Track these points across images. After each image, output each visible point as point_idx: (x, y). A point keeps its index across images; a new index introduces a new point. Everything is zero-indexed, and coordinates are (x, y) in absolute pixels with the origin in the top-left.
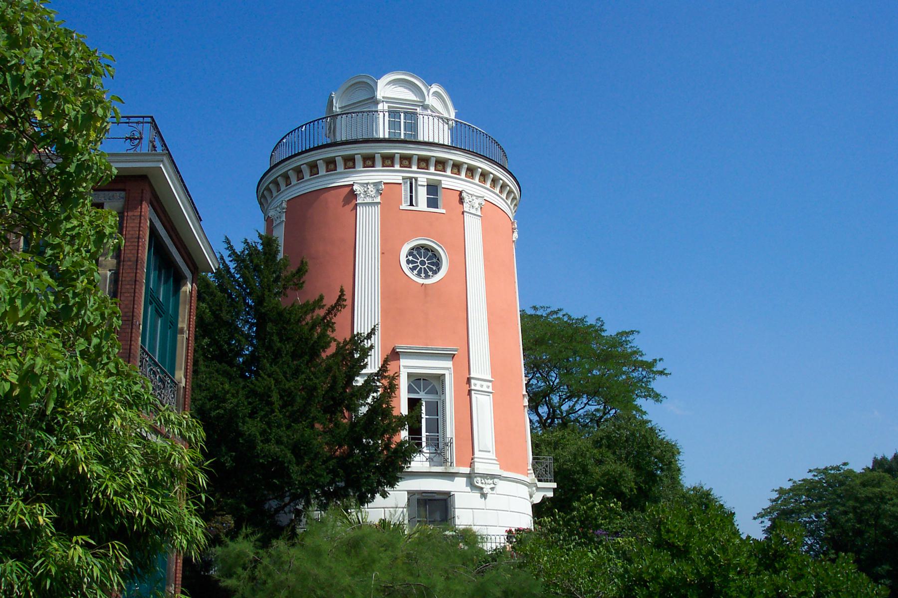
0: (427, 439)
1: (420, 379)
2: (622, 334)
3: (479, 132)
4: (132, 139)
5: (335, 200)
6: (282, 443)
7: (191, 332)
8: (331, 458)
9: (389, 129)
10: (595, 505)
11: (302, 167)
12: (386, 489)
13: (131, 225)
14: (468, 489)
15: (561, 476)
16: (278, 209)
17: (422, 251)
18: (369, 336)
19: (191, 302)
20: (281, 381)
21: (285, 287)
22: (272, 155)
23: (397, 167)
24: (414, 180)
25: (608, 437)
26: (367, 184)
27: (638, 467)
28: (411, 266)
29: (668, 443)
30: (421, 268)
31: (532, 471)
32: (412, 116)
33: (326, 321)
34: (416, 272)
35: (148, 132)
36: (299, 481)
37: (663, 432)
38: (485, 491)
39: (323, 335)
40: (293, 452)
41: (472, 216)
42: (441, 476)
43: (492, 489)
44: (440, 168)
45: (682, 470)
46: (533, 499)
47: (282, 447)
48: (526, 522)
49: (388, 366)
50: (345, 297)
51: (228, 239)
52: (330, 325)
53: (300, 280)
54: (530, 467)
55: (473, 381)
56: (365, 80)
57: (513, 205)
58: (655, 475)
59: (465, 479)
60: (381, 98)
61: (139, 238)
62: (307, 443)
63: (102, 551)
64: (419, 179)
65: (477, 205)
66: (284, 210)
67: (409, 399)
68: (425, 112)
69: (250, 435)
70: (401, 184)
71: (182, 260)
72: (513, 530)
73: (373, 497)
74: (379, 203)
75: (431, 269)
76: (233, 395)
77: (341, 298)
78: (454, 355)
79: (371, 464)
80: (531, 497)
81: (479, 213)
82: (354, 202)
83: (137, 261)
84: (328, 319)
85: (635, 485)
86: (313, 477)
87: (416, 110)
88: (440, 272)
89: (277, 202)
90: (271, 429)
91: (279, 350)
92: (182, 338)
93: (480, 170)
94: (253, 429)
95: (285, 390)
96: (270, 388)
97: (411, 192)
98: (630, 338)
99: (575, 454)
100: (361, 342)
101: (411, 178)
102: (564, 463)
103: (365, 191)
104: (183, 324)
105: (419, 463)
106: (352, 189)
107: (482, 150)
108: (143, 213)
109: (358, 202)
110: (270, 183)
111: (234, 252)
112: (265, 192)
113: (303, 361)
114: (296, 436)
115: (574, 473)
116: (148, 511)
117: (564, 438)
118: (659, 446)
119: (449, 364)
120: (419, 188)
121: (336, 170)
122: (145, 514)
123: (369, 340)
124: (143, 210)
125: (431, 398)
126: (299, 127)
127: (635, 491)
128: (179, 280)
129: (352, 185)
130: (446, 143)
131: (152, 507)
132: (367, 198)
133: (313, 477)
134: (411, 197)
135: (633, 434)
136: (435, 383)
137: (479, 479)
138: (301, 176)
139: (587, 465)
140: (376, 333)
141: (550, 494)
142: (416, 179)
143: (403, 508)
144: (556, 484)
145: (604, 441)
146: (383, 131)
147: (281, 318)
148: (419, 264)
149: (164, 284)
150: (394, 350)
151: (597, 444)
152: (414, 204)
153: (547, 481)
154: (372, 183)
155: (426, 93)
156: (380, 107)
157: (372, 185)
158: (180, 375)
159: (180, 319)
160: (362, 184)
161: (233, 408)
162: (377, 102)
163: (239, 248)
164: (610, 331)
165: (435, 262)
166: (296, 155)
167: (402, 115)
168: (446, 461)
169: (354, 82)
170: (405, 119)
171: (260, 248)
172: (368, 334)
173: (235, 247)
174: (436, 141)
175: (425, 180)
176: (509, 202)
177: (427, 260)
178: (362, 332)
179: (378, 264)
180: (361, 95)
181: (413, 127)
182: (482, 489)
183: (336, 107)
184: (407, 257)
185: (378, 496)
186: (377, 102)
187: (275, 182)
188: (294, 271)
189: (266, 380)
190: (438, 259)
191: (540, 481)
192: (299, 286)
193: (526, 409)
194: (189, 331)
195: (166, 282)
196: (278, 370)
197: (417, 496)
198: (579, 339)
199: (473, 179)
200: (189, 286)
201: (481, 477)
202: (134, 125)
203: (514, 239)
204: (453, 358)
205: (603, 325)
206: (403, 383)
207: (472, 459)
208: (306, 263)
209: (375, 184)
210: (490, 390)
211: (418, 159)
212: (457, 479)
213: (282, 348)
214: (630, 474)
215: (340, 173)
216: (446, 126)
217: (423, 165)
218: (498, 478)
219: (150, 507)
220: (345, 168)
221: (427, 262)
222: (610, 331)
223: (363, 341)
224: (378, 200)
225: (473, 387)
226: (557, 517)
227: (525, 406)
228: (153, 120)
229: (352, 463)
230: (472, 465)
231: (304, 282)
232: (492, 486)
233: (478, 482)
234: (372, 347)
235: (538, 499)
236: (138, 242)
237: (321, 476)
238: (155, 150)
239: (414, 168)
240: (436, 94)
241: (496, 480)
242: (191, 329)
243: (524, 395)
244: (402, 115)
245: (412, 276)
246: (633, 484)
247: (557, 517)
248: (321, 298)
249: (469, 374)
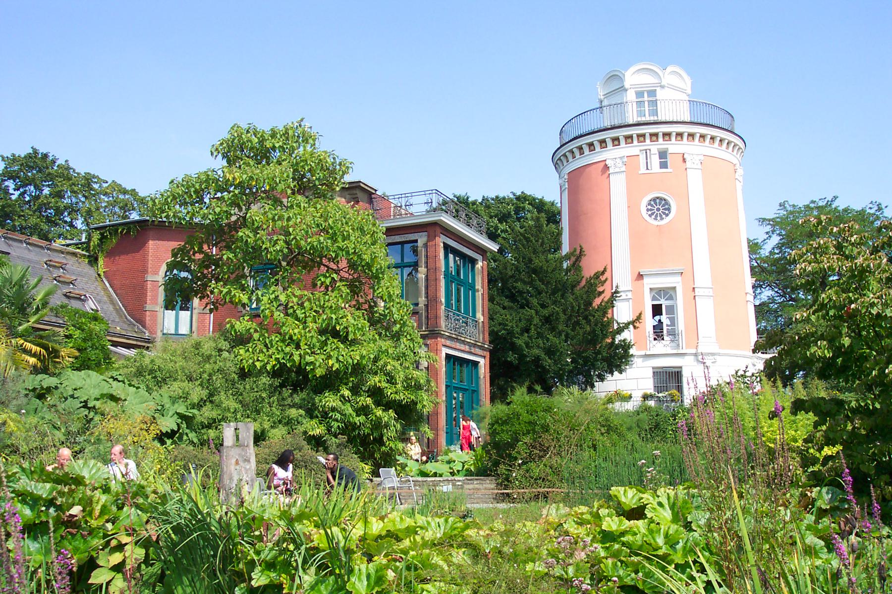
5: (596, 171)
14: (696, 363)
56: (614, 73)
75: (664, 213)
92: (479, 295)
97: (647, 159)
101: (646, 150)
104: (478, 286)
119: (678, 279)
125: (669, 303)
128: (473, 262)
134: (647, 163)
136: (672, 292)
142: (650, 150)
155: (662, 76)
167: (646, 95)
179: (626, 214)
180: (615, 85)
209: (621, 158)
212: (686, 357)
215: (599, 152)
217: (654, 138)
224: (623, 169)
244: (646, 95)
245: (651, 221)
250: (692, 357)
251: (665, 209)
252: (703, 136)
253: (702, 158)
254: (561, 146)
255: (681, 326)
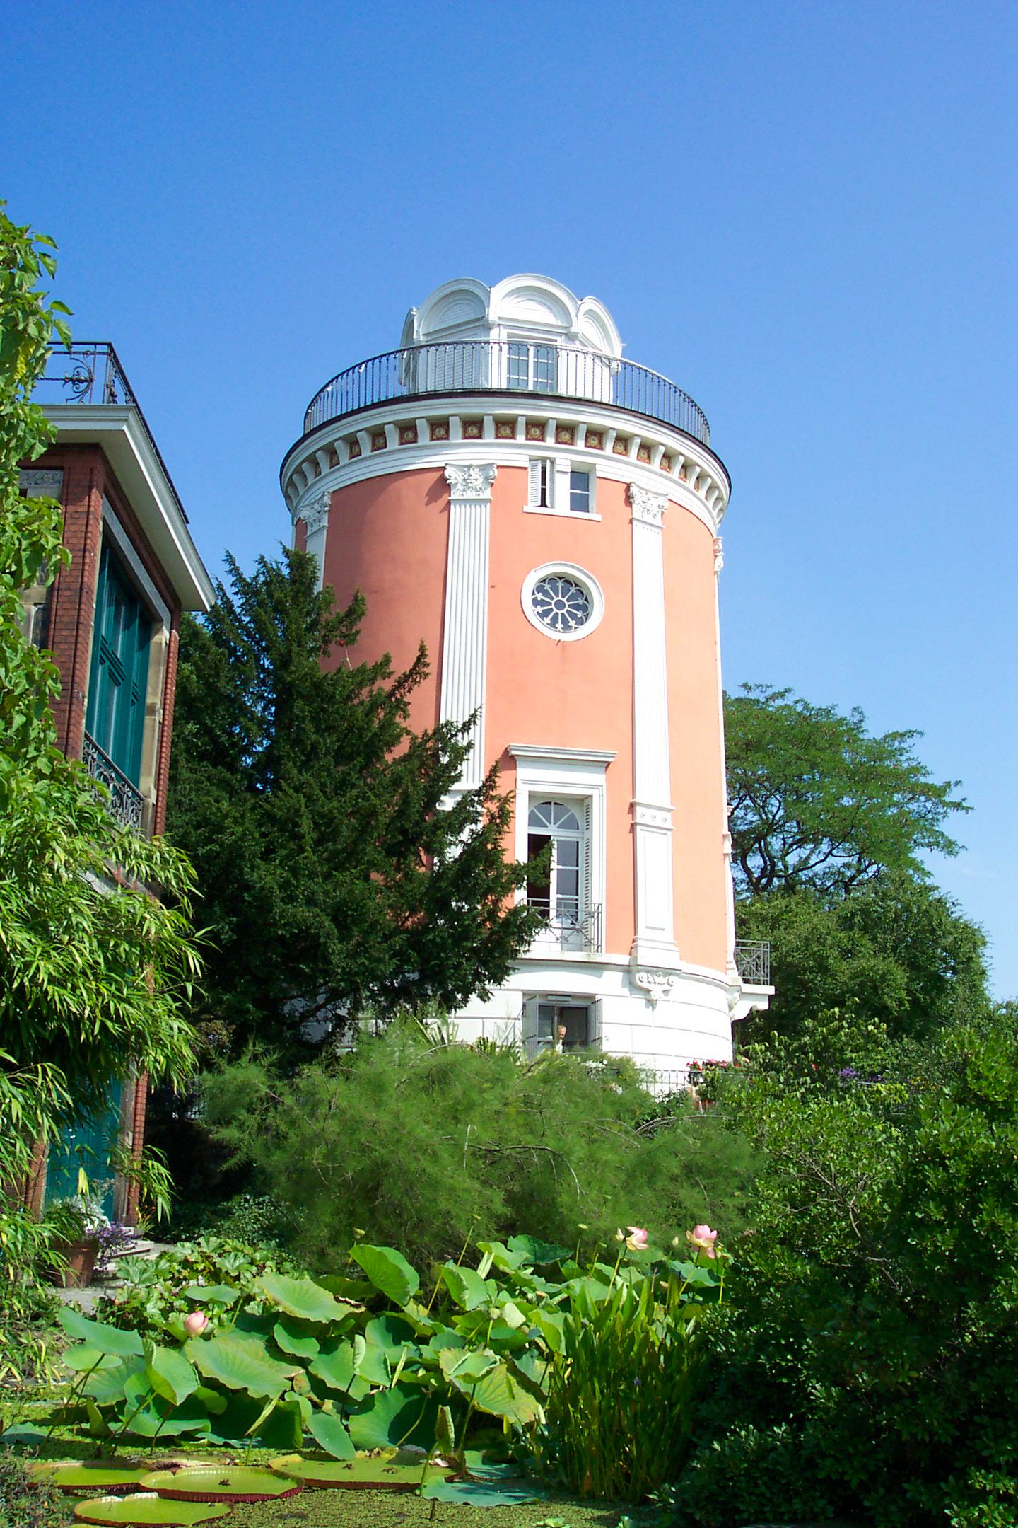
0: (559, 905)
1: (550, 803)
2: (894, 736)
3: (662, 383)
4: (75, 381)
5: (412, 494)
6: (316, 905)
7: (167, 712)
8: (397, 931)
9: (509, 373)
10: (842, 1027)
11: (358, 434)
12: (487, 987)
13: (72, 528)
14: (626, 991)
15: (782, 974)
16: (316, 506)
17: (560, 584)
18: (466, 727)
19: (168, 662)
20: (318, 799)
21: (326, 641)
22: (307, 413)
23: (521, 438)
24: (548, 462)
25: (865, 913)
26: (469, 467)
27: (913, 966)
28: (540, 609)
29: (966, 926)
30: (557, 613)
31: (734, 965)
32: (548, 350)
33: (393, 699)
34: (547, 620)
35: (102, 370)
36: (343, 969)
37: (959, 907)
38: (654, 995)
39: (388, 724)
40: (334, 920)
41: (646, 526)
42: (580, 967)
43: (666, 992)
44: (595, 442)
45: (989, 973)
46: (733, 1012)
47: (316, 910)
48: (722, 1050)
49: (497, 780)
50: (427, 660)
51: (231, 556)
52: (401, 706)
53: (351, 629)
54: (731, 958)
55: (639, 810)
57: (717, 510)
58: (941, 979)
59: (621, 974)
60: (496, 320)
61: (85, 551)
62: (358, 905)
63: (27, 1076)
64: (557, 461)
65: (655, 509)
66: (327, 509)
67: (530, 836)
68: (571, 346)
69: (262, 888)
70: (526, 468)
71: (155, 590)
72: (700, 1063)
73: (465, 1000)
74: (489, 500)
75: (573, 616)
76: (235, 822)
77: (420, 661)
78: (609, 763)
79: (465, 944)
80: (731, 1008)
81: (658, 522)
82: (445, 498)
83: (81, 589)
84: (398, 696)
85: (908, 995)
86: (367, 963)
87: (556, 341)
88: (589, 621)
89: (314, 494)
90: (297, 880)
91: (314, 747)
92: (152, 723)
93: (662, 449)
94: (269, 878)
95: (322, 816)
96: (298, 811)
97: (544, 482)
98: (910, 742)
99: (807, 939)
100: (452, 736)
101: (544, 460)
102: (788, 954)
103: (465, 480)
104: (154, 697)
105: (543, 944)
106: (443, 474)
107: (666, 412)
108: (92, 509)
109: (453, 497)
110: (303, 462)
111: (240, 579)
112: (294, 477)
113: (355, 765)
114: (341, 893)
115: (805, 970)
116: (105, 1011)
117: (790, 911)
118: (952, 930)
119: (598, 778)
120: (558, 476)
121: (416, 442)
122: (99, 1015)
123: (466, 734)
124: (92, 503)
126: (355, 367)
127: (907, 1005)
128: (149, 623)
129: (444, 468)
130: (605, 401)
131: (112, 1004)
132: (469, 491)
133: (367, 963)
134: (543, 491)
135: (907, 909)
136: (575, 811)
137: (644, 975)
138: (355, 450)
139: (828, 957)
140: (478, 722)
141: (763, 1005)
142: (553, 462)
143: (515, 1019)
144: (773, 988)
145: (857, 919)
146: (498, 378)
147: (318, 690)
148: (553, 606)
149: (124, 630)
150: (506, 752)
151: (846, 922)
152: (548, 503)
153: (758, 982)
154: (478, 466)
155: (573, 313)
156: (494, 334)
157: (477, 470)
158: (147, 785)
159: (149, 689)
160: (460, 467)
161: (236, 842)
162: (488, 327)
163: (249, 571)
164: (874, 730)
165: (583, 606)
166: (348, 414)
167: (532, 349)
168: (589, 942)
169: (446, 292)
170: (536, 356)
171: (285, 571)
172: (464, 724)
173: (241, 570)
174: (589, 396)
175: (569, 463)
176: (710, 503)
177: (568, 600)
178: (454, 720)
179: (484, 606)
180: (462, 313)
181: (549, 371)
182: (648, 991)
183: (418, 334)
184: (533, 594)
185: (473, 997)
186: (488, 327)
187: (313, 460)
188: (342, 614)
189: (291, 796)
190: (586, 600)
191: (746, 981)
192: (349, 639)
193: (729, 859)
194: (164, 709)
195: (127, 627)
196: (312, 780)
197: (538, 1001)
198: (822, 743)
199: (649, 463)
200: (166, 633)
201: (648, 972)
202: (80, 357)
203: (717, 569)
204: (607, 767)
205: (862, 721)
206: (521, 810)
207: (634, 941)
208: (363, 599)
209: (483, 468)
210: (668, 825)
211: (558, 427)
212: (606, 974)
213: (319, 743)
214: (900, 975)
216: (606, 370)
217: (565, 436)
218: (678, 975)
219: (108, 1003)
220: (432, 440)
221: (567, 604)
222: (874, 730)
223: (456, 735)
224: (487, 494)
225: (638, 820)
226: (777, 1044)
227: (725, 855)
228: (112, 350)
229: (433, 941)
230: (632, 951)
231: (358, 632)
232: (667, 987)
233: (642, 978)
234: (470, 746)
235: (741, 1013)
236: (84, 557)
237: (380, 960)
238: (114, 401)
239: (550, 441)
240: (591, 314)
241: (672, 978)
242: (167, 707)
243: (724, 836)
244: (532, 349)
245: (542, 626)
246: (904, 993)
247: (777, 1044)
248: (387, 660)
249: (634, 796)
250: (620, 975)
251: (577, 607)
252: (668, 457)
253: (667, 504)
254: (305, 437)
255: (598, 890)
